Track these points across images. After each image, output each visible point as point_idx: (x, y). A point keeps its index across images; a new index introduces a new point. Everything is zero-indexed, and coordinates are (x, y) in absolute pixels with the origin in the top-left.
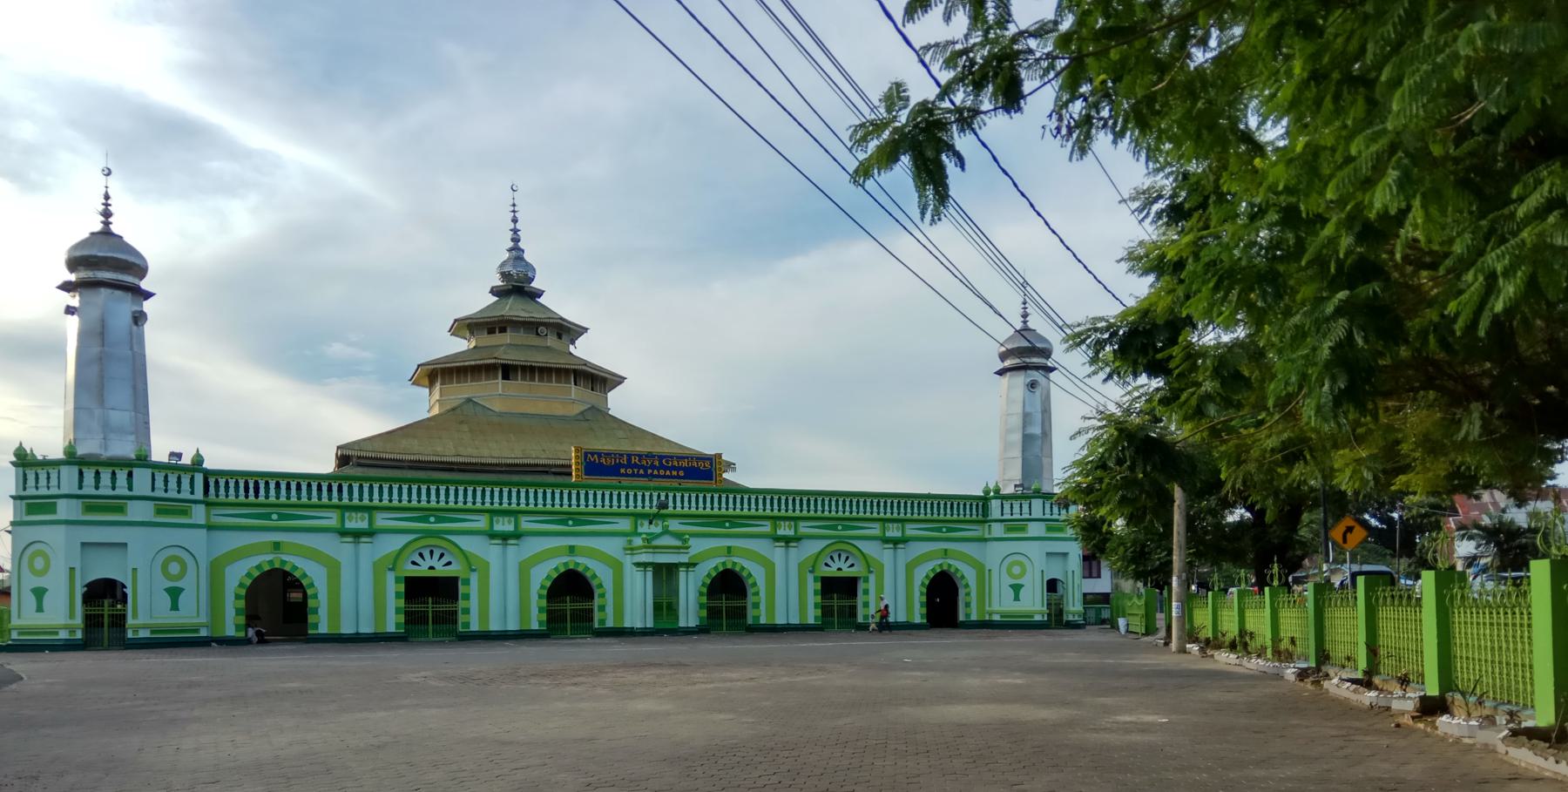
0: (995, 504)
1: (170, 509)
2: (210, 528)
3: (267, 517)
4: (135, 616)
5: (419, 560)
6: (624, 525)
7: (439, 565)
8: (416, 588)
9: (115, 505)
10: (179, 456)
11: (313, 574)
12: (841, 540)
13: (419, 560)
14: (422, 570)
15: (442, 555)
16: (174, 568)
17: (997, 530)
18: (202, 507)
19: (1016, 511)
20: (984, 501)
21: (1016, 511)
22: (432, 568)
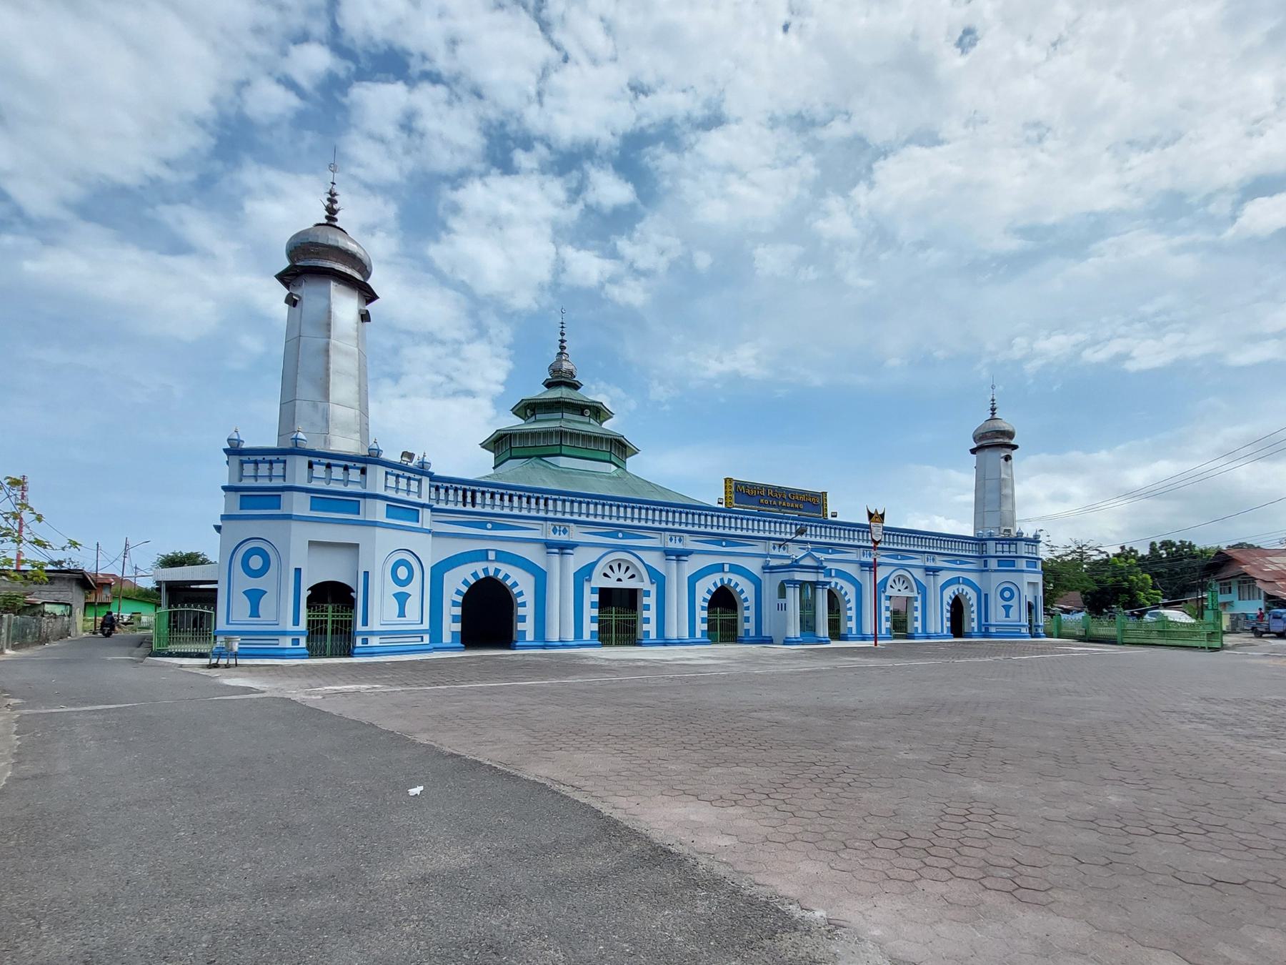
0: (991, 544)
1: (403, 510)
2: (436, 534)
3: (482, 525)
4: (365, 623)
5: (609, 572)
6: (759, 548)
7: (625, 577)
8: (607, 598)
9: (349, 502)
10: (411, 456)
11: (521, 583)
12: (903, 567)
13: (609, 572)
14: (611, 583)
15: (628, 569)
16: (402, 573)
17: (993, 564)
18: (427, 512)
19: (1006, 550)
20: (979, 541)
21: (1006, 550)
22: (619, 580)
